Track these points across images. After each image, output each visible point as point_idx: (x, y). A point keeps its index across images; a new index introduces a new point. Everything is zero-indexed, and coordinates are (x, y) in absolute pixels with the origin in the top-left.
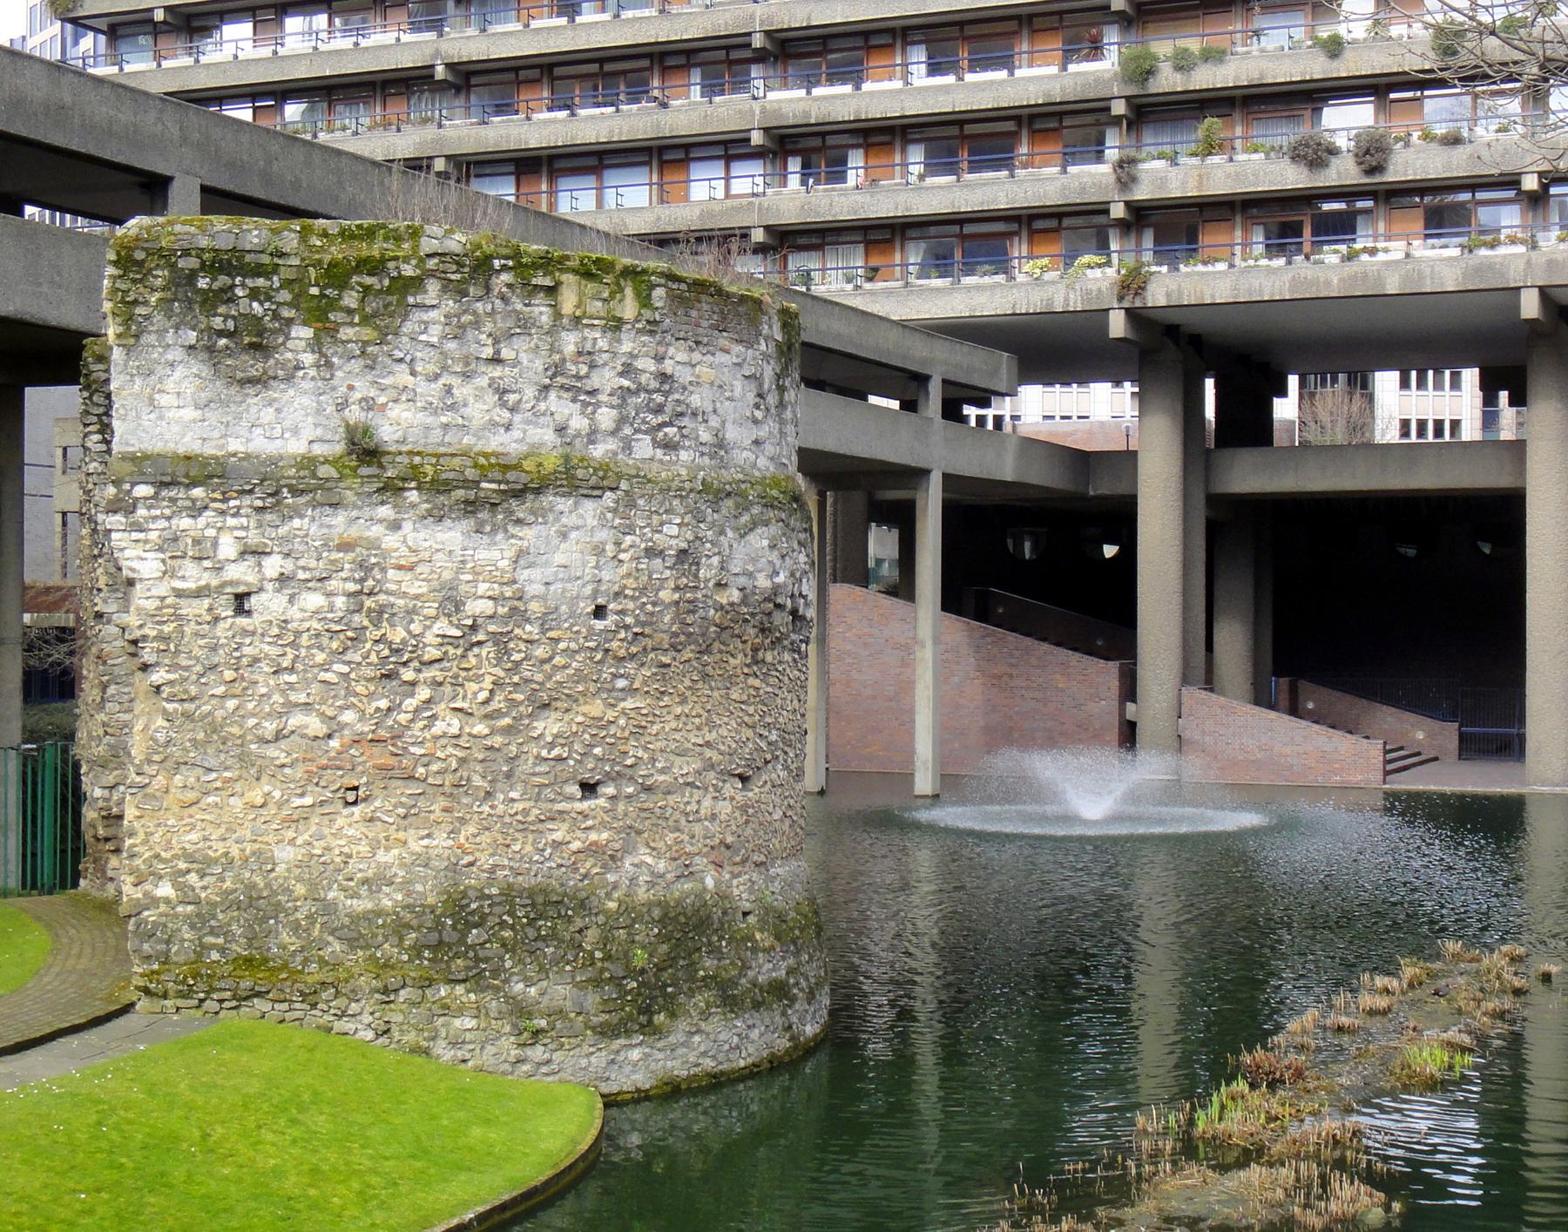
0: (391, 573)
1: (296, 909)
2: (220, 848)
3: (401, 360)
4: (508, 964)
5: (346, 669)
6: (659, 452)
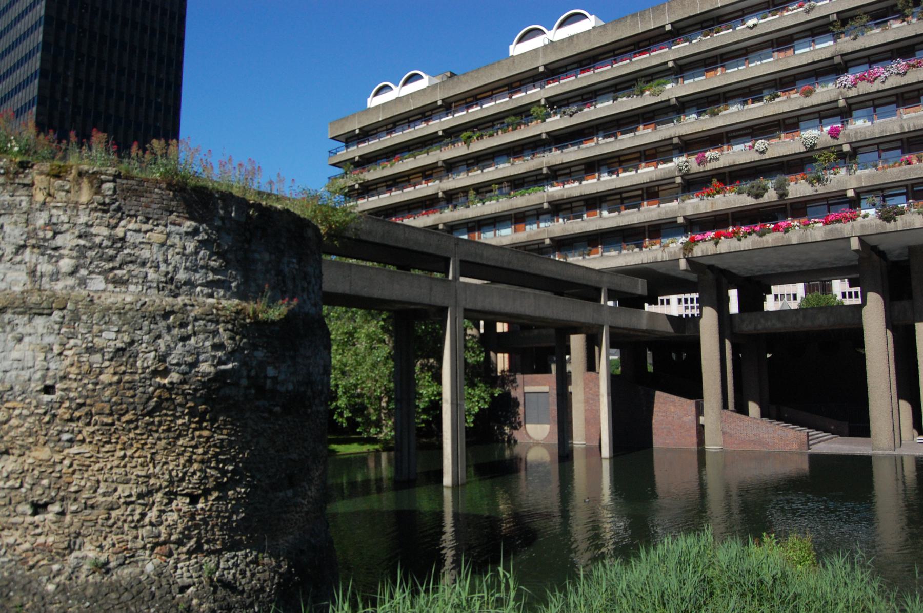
6: (111, 287)
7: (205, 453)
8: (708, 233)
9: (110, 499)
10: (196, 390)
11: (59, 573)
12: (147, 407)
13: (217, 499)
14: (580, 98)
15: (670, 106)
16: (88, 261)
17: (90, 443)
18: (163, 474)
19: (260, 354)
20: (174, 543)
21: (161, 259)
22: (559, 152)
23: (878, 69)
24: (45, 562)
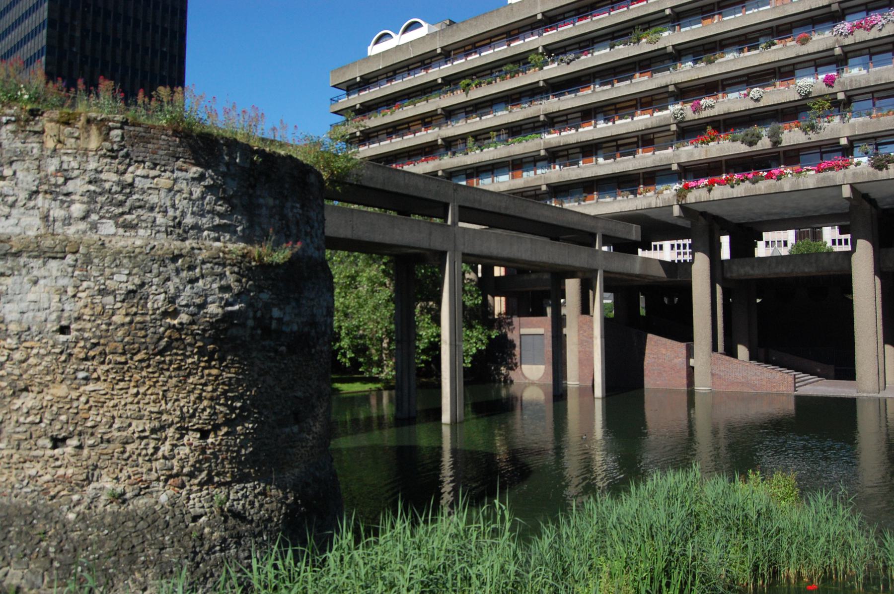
6: (121, 231)
7: (214, 390)
9: (125, 434)
10: (204, 331)
11: (79, 502)
12: (159, 347)
13: (227, 434)
16: (99, 206)
17: (105, 380)
18: (175, 410)
19: (265, 296)
20: (187, 475)
21: (168, 204)
22: (556, 99)
23: (875, 17)
24: (65, 492)
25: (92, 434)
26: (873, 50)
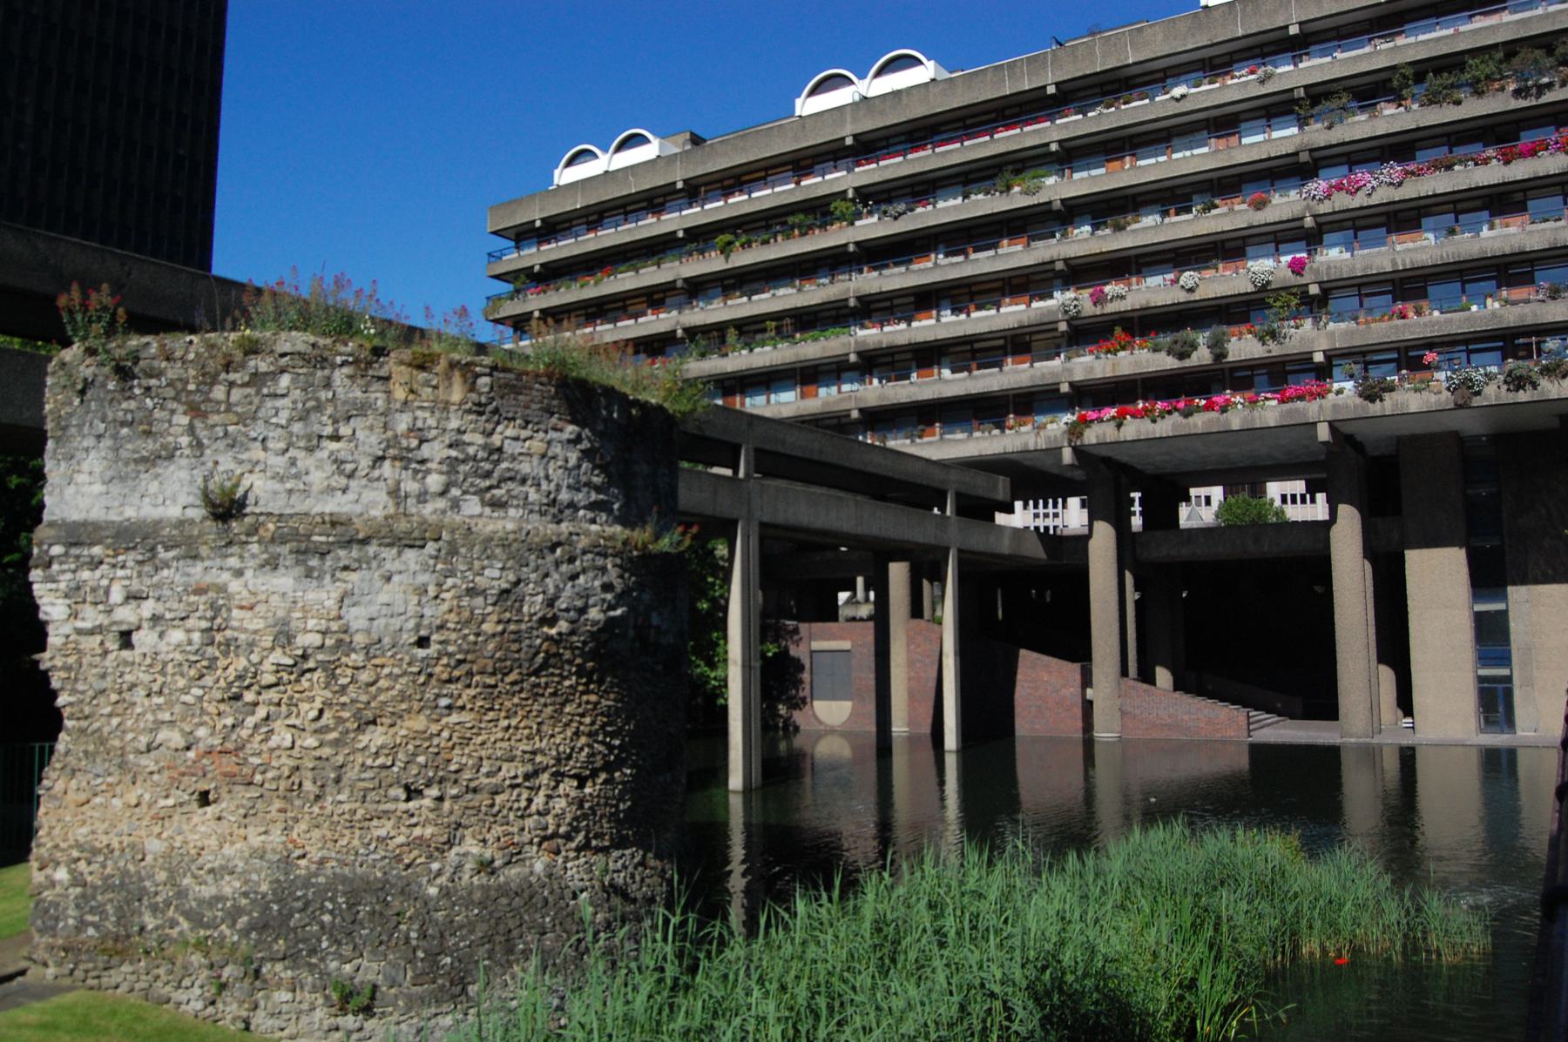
0: (236, 613)
1: (156, 894)
2: (105, 840)
3: (255, 439)
4: (325, 945)
5: (200, 692)
6: (488, 510)
7: (593, 723)
8: (1106, 409)
9: (494, 780)
10: (585, 643)
11: (439, 873)
13: (605, 782)
14: (909, 190)
15: (1051, 211)
19: (646, 597)
20: (562, 837)
21: (542, 474)
22: (875, 274)
23: (1362, 175)
24: (422, 860)
25: (456, 782)
26: (1359, 223)
